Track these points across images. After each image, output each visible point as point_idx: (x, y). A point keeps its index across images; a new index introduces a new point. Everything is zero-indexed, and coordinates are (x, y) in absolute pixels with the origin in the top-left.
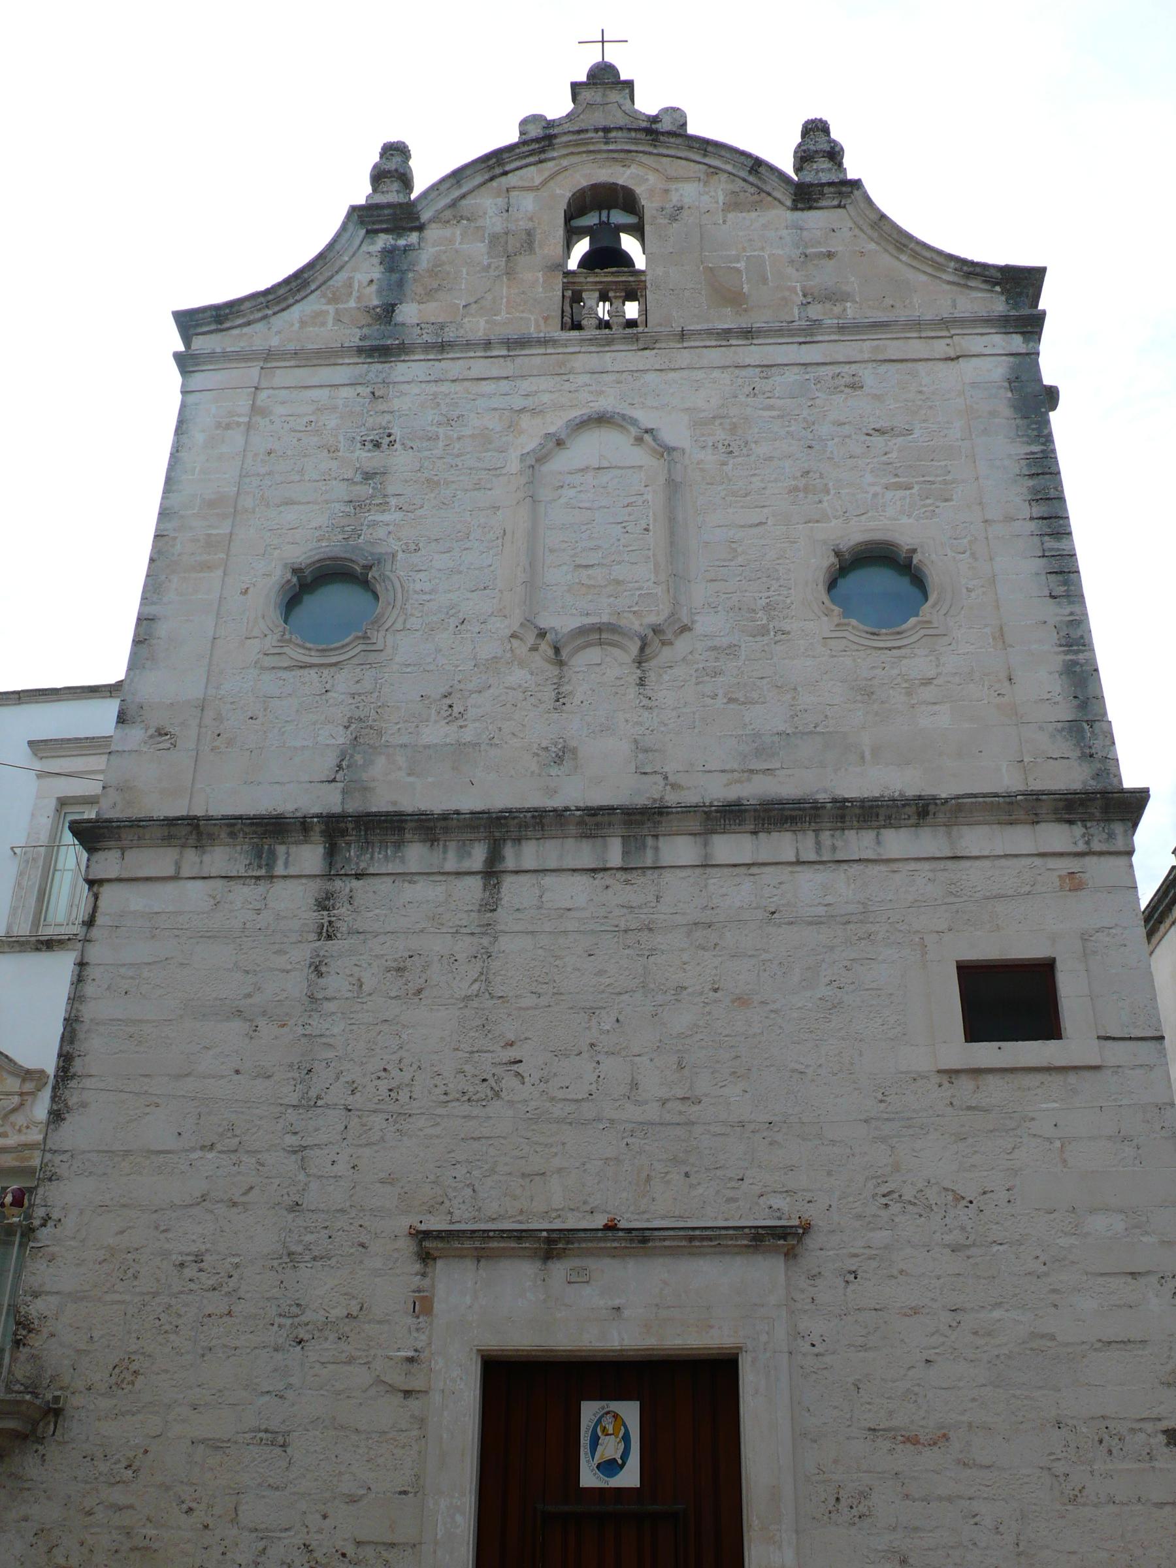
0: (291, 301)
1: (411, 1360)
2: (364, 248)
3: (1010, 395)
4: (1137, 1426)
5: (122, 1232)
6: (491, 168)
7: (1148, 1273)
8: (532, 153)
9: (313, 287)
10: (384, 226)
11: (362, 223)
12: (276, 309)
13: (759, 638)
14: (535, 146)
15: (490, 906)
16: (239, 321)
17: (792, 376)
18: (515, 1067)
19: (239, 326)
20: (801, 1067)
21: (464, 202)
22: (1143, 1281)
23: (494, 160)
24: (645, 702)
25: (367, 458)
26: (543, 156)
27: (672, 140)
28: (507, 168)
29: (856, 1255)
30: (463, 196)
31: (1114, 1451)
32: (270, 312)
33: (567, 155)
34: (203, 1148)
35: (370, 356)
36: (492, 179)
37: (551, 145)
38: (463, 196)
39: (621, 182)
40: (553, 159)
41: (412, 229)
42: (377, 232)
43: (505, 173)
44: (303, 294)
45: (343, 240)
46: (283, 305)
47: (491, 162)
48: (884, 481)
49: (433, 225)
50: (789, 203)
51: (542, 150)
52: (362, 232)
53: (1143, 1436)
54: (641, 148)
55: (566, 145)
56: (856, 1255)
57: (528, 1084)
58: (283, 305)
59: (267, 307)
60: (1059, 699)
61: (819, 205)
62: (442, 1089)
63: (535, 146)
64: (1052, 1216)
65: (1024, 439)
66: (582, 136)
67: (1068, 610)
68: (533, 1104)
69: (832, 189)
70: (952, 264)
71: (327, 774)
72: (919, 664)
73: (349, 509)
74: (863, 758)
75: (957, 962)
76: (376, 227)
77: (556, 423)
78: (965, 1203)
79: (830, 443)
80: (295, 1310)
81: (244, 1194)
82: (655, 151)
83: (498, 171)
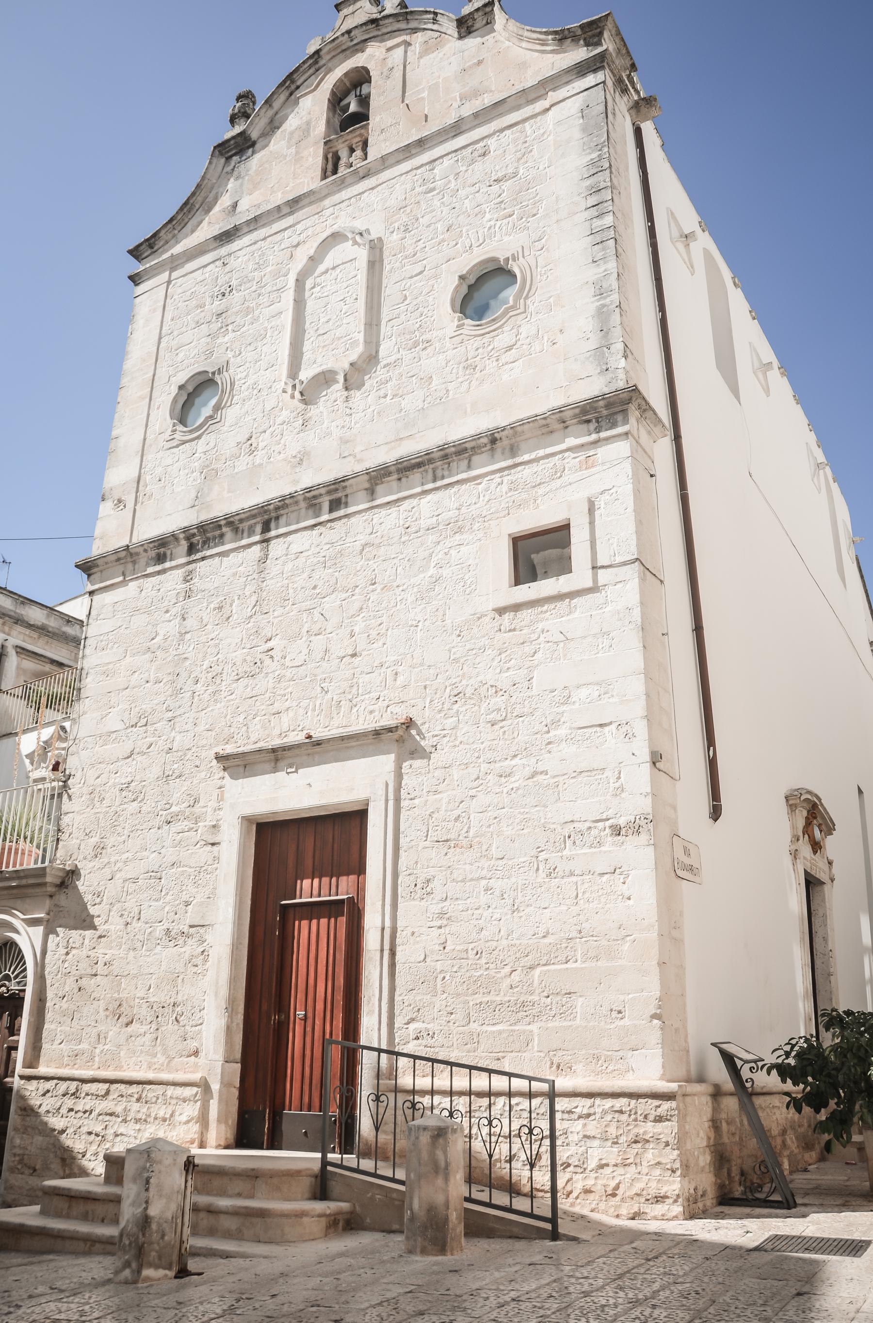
0: (186, 220)
1: (214, 826)
2: (225, 170)
3: (581, 121)
4: (592, 825)
5: (98, 777)
6: (288, 87)
7: (611, 723)
8: (310, 67)
9: (197, 207)
10: (234, 152)
11: (221, 154)
12: (179, 228)
13: (413, 350)
14: (311, 61)
15: (263, 560)
16: (161, 243)
17: (447, 162)
18: (270, 653)
19: (163, 246)
20: (414, 623)
21: (277, 116)
22: (607, 729)
23: (288, 82)
24: (348, 411)
25: (218, 305)
26: (317, 66)
27: (387, 21)
28: (298, 83)
29: (436, 736)
30: (276, 113)
31: (577, 842)
32: (176, 232)
33: (331, 58)
34: (132, 726)
35: (222, 240)
36: (291, 94)
37: (319, 57)
38: (276, 113)
39: (360, 65)
40: (324, 65)
41: (248, 148)
42: (231, 157)
43: (298, 87)
44: (192, 213)
45: (211, 171)
46: (182, 225)
47: (287, 84)
48: (496, 216)
49: (261, 139)
50: (456, 35)
51: (316, 62)
52: (223, 160)
53: (597, 831)
54: (371, 35)
55: (329, 52)
56: (436, 736)
57: (275, 661)
58: (182, 225)
59: (174, 229)
60: (590, 335)
61: (475, 28)
62: (235, 673)
63: (311, 61)
64: (554, 694)
65: (588, 151)
66: (336, 42)
67: (603, 269)
68: (277, 673)
69: (480, 13)
70: (550, 37)
71: (191, 503)
72: (504, 338)
73: (209, 339)
74: (466, 412)
75: (509, 535)
76: (230, 154)
77: (310, 249)
78: (501, 693)
79: (466, 201)
80: (167, 806)
81: (149, 748)
82: (380, 33)
83: (293, 87)
